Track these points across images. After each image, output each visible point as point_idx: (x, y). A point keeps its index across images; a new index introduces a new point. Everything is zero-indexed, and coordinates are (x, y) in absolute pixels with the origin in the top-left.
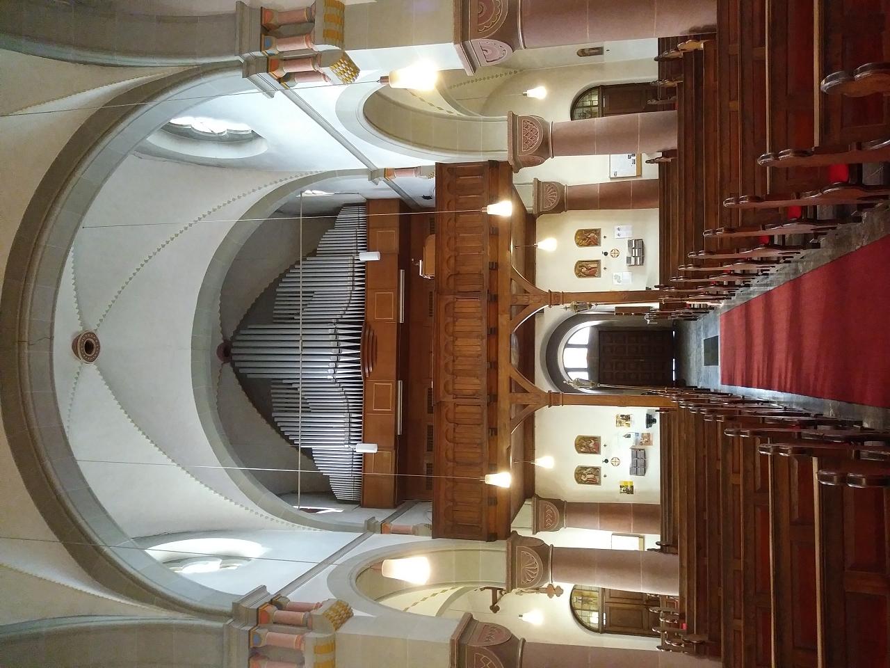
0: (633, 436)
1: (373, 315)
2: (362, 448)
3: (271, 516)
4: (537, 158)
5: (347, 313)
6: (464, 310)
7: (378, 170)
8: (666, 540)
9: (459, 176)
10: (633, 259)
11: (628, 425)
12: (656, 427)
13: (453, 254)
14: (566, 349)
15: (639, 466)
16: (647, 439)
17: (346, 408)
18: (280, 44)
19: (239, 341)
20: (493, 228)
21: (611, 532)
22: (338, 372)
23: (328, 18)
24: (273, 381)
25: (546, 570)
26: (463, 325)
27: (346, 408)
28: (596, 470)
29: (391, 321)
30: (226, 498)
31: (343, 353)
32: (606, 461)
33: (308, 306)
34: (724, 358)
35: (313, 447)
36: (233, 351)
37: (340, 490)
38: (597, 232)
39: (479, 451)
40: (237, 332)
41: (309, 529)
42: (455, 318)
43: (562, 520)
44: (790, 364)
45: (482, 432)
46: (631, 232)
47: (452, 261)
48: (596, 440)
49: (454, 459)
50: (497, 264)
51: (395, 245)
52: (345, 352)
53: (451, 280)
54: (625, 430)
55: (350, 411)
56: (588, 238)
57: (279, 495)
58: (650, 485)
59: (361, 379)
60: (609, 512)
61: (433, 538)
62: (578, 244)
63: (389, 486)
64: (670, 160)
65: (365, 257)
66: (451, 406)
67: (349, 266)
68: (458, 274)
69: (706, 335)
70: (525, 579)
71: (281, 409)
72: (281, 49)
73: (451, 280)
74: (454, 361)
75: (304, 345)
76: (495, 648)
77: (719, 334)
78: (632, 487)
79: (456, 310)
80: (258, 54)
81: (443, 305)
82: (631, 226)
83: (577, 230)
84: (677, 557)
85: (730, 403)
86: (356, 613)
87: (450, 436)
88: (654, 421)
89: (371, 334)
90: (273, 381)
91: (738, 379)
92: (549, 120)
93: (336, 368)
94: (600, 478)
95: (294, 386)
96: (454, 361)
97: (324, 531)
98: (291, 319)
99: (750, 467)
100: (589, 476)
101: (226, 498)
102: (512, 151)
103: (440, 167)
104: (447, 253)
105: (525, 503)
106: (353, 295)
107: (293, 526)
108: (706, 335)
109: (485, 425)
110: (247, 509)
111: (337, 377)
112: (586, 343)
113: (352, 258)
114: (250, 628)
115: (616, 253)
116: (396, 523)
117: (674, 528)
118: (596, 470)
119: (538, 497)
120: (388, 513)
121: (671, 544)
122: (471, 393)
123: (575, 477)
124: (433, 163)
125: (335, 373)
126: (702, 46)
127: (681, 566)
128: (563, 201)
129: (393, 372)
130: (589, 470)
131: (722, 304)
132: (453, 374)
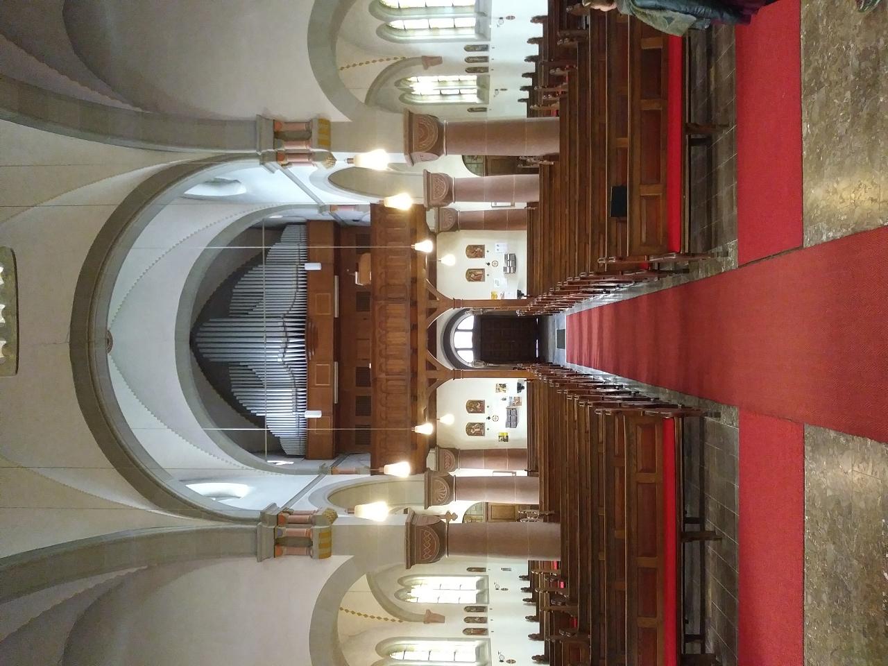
3: (245, 467)
5: (293, 309)
7: (325, 206)
10: (508, 269)
12: (524, 392)
14: (457, 333)
15: (512, 421)
16: (518, 402)
18: (287, 145)
20: (415, 255)
23: (320, 131)
25: (451, 492)
26: (391, 322)
28: (482, 425)
30: (210, 454)
31: (291, 341)
32: (489, 418)
35: (268, 415)
38: (482, 247)
42: (387, 317)
43: (457, 463)
46: (506, 248)
47: (383, 276)
48: (482, 403)
49: (386, 417)
52: (292, 340)
54: (502, 394)
56: (476, 252)
58: (520, 434)
60: (492, 455)
61: (372, 475)
62: (468, 256)
63: (328, 444)
64: (534, 208)
68: (388, 284)
70: (437, 499)
72: (287, 148)
74: (386, 349)
76: (432, 526)
78: (507, 436)
80: (273, 150)
81: (377, 308)
82: (506, 244)
85: (567, 375)
86: (339, 516)
88: (523, 388)
91: (575, 360)
92: (452, 175)
95: (250, 367)
97: (288, 476)
98: (245, 314)
100: (476, 429)
101: (210, 454)
103: (373, 206)
104: (380, 270)
105: (431, 451)
110: (227, 461)
112: (471, 327)
114: (274, 527)
115: (496, 264)
116: (340, 467)
118: (482, 425)
120: (334, 461)
126: (553, 163)
127: (540, 482)
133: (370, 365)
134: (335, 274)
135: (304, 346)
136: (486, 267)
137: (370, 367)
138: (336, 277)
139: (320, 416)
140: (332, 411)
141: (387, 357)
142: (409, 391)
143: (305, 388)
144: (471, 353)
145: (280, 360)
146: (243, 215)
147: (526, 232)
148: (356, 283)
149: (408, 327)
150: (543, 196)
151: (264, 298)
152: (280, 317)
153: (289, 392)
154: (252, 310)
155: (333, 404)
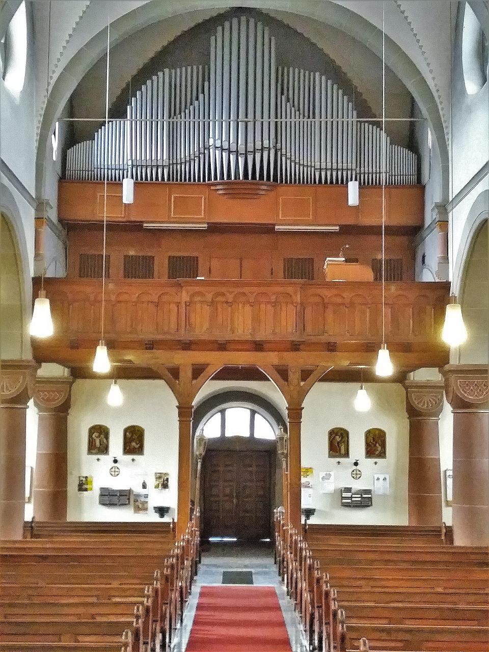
0: (143, 492)
1: (286, 193)
2: (128, 186)
4: (451, 395)
5: (288, 161)
6: (283, 314)
8: (38, 527)
9: (434, 308)
10: (349, 495)
11: (157, 487)
12: (155, 518)
13: (347, 301)
14: (249, 411)
15: (111, 498)
16: (141, 507)
20: (371, 349)
21: (34, 467)
22: (217, 152)
28: (104, 450)
30: (70, 36)
31: (239, 158)
32: (115, 461)
33: (297, 113)
34: (224, 589)
35: (128, 123)
37: (78, 152)
38: (382, 455)
41: (37, 134)
42: (275, 304)
43: (46, 410)
44: (215, 637)
46: (381, 492)
47: (339, 300)
48: (139, 450)
49: (120, 302)
51: (367, 220)
52: (241, 161)
53: (318, 299)
54: (151, 482)
55: (171, 167)
63: (82, 213)
64: (443, 538)
65: (353, 188)
66: (177, 299)
67: (345, 165)
68: (325, 306)
69: (257, 573)
71: (173, 90)
73: (318, 299)
74: (227, 302)
77: (255, 585)
78: (86, 490)
79: (284, 305)
81: (290, 290)
82: (388, 492)
83: (386, 431)
84: (20, 538)
85: (181, 588)
87: (145, 298)
88: (162, 516)
89: (263, 192)
91: (205, 600)
94: (96, 454)
95: (201, 96)
96: (227, 302)
97: (35, 151)
98: (282, 89)
99: (128, 593)
102: (459, 369)
103: (446, 286)
104: (348, 295)
105: (66, 369)
106: (309, 169)
108: (257, 573)
109: (154, 337)
111: (211, 150)
112: (257, 435)
113: (354, 167)
115: (356, 475)
116: (47, 233)
117: (52, 536)
118: (104, 450)
119: (73, 382)
121: (35, 532)
122: (192, 320)
123: (96, 426)
124: (451, 279)
128: (420, 416)
129: (221, 218)
130: (105, 441)
131: (285, 588)
133: (203, 278)
134: (342, 227)
135: (233, 178)
137: (198, 278)
138: (337, 228)
139: (125, 201)
141: (212, 303)
142: (160, 337)
143: (169, 179)
144: (217, 434)
145: (211, 141)
146: (434, 91)
147: (407, 524)
148: (328, 259)
150: (464, 552)
151: (306, 120)
152: (277, 143)
153: (163, 156)
154: (288, 100)
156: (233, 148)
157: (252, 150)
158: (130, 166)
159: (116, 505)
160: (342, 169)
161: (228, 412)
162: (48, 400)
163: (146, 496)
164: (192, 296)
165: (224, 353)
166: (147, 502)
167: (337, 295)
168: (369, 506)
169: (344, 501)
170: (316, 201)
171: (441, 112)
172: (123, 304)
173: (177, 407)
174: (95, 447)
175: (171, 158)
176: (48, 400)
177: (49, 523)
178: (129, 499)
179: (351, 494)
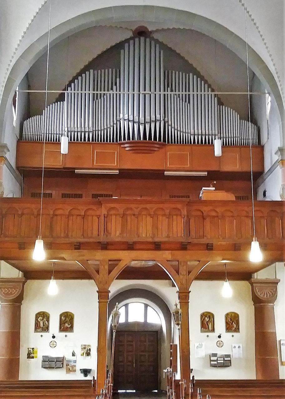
1: (171, 150)
2: (64, 142)
3: (10, 69)
5: (173, 130)
6: (175, 223)
10: (215, 358)
12: (81, 377)
13: (220, 214)
17: (97, 129)
19: (151, 42)
24: (118, 70)
26: (163, 222)
27: (97, 129)
28: (46, 329)
29: (166, 164)
31: (141, 126)
33: (178, 99)
35: (65, 103)
36: (142, 39)
37: (31, 124)
38: (237, 330)
39: (62, 235)
40: (157, 41)
42: (169, 216)
43: (7, 301)
45: (77, 237)
46: (237, 356)
47: (214, 214)
48: (70, 329)
50: (212, 249)
51: (228, 168)
54: (79, 352)
55: (94, 132)
57: (27, 75)
59: (120, 141)
62: (227, 315)
65: (218, 145)
66: (98, 213)
68: (204, 218)
73: (199, 213)
74: (134, 215)
75: (147, 95)
78: (33, 358)
79: (175, 217)
81: (179, 206)
82: (242, 356)
83: (239, 313)
87: (75, 212)
88: (86, 375)
90: (118, 70)
93: (129, 121)
95: (114, 87)
96: (134, 215)
98: (168, 85)
105: (20, 272)
107: (3, 86)
112: (149, 321)
115: (220, 345)
118: (46, 329)
120: (13, 163)
123: (41, 312)
125: (124, 120)
130: (47, 322)
132: (124, 215)
133: (117, 198)
134: (208, 172)
136: (217, 333)
137: (113, 198)
139: (62, 152)
140: (68, 165)
141: (124, 216)
148: (203, 188)
149: (161, 237)
151: (187, 93)
155: (75, 169)
156: (136, 119)
157: (149, 121)
158: (67, 132)
159: (54, 368)
160: (209, 135)
161: (130, 306)
162: (7, 294)
163: (75, 362)
164: (109, 210)
165: (132, 251)
166: (75, 366)
167: (211, 210)
168: (229, 366)
169: (212, 363)
170: (191, 154)
171: (280, 88)
172: (59, 217)
173: (97, 292)
174: (40, 327)
175: (94, 127)
176: (7, 294)
177: (6, 381)
178: (63, 364)
179: (216, 358)
